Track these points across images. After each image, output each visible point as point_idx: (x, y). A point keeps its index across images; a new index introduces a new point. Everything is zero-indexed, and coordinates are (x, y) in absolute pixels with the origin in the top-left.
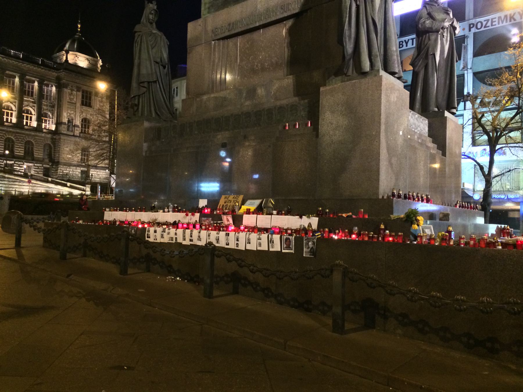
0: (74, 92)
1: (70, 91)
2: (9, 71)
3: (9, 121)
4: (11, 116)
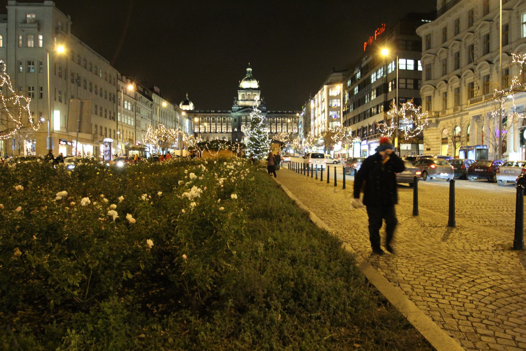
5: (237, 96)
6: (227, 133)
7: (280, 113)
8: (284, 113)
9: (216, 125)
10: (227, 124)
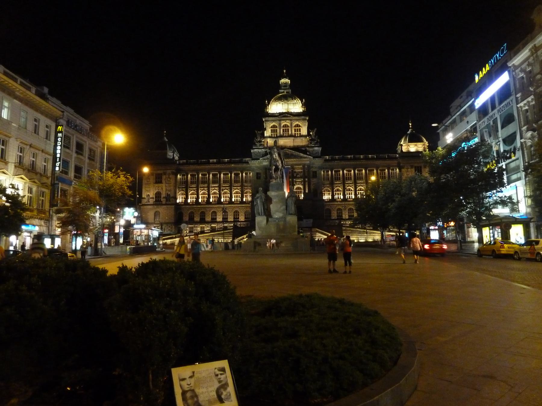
0: (409, 170)
1: (406, 170)
2: (368, 168)
4: (352, 194)
6: (242, 202)
7: (351, 159)
8: (359, 159)
9: (219, 187)
10: (242, 187)
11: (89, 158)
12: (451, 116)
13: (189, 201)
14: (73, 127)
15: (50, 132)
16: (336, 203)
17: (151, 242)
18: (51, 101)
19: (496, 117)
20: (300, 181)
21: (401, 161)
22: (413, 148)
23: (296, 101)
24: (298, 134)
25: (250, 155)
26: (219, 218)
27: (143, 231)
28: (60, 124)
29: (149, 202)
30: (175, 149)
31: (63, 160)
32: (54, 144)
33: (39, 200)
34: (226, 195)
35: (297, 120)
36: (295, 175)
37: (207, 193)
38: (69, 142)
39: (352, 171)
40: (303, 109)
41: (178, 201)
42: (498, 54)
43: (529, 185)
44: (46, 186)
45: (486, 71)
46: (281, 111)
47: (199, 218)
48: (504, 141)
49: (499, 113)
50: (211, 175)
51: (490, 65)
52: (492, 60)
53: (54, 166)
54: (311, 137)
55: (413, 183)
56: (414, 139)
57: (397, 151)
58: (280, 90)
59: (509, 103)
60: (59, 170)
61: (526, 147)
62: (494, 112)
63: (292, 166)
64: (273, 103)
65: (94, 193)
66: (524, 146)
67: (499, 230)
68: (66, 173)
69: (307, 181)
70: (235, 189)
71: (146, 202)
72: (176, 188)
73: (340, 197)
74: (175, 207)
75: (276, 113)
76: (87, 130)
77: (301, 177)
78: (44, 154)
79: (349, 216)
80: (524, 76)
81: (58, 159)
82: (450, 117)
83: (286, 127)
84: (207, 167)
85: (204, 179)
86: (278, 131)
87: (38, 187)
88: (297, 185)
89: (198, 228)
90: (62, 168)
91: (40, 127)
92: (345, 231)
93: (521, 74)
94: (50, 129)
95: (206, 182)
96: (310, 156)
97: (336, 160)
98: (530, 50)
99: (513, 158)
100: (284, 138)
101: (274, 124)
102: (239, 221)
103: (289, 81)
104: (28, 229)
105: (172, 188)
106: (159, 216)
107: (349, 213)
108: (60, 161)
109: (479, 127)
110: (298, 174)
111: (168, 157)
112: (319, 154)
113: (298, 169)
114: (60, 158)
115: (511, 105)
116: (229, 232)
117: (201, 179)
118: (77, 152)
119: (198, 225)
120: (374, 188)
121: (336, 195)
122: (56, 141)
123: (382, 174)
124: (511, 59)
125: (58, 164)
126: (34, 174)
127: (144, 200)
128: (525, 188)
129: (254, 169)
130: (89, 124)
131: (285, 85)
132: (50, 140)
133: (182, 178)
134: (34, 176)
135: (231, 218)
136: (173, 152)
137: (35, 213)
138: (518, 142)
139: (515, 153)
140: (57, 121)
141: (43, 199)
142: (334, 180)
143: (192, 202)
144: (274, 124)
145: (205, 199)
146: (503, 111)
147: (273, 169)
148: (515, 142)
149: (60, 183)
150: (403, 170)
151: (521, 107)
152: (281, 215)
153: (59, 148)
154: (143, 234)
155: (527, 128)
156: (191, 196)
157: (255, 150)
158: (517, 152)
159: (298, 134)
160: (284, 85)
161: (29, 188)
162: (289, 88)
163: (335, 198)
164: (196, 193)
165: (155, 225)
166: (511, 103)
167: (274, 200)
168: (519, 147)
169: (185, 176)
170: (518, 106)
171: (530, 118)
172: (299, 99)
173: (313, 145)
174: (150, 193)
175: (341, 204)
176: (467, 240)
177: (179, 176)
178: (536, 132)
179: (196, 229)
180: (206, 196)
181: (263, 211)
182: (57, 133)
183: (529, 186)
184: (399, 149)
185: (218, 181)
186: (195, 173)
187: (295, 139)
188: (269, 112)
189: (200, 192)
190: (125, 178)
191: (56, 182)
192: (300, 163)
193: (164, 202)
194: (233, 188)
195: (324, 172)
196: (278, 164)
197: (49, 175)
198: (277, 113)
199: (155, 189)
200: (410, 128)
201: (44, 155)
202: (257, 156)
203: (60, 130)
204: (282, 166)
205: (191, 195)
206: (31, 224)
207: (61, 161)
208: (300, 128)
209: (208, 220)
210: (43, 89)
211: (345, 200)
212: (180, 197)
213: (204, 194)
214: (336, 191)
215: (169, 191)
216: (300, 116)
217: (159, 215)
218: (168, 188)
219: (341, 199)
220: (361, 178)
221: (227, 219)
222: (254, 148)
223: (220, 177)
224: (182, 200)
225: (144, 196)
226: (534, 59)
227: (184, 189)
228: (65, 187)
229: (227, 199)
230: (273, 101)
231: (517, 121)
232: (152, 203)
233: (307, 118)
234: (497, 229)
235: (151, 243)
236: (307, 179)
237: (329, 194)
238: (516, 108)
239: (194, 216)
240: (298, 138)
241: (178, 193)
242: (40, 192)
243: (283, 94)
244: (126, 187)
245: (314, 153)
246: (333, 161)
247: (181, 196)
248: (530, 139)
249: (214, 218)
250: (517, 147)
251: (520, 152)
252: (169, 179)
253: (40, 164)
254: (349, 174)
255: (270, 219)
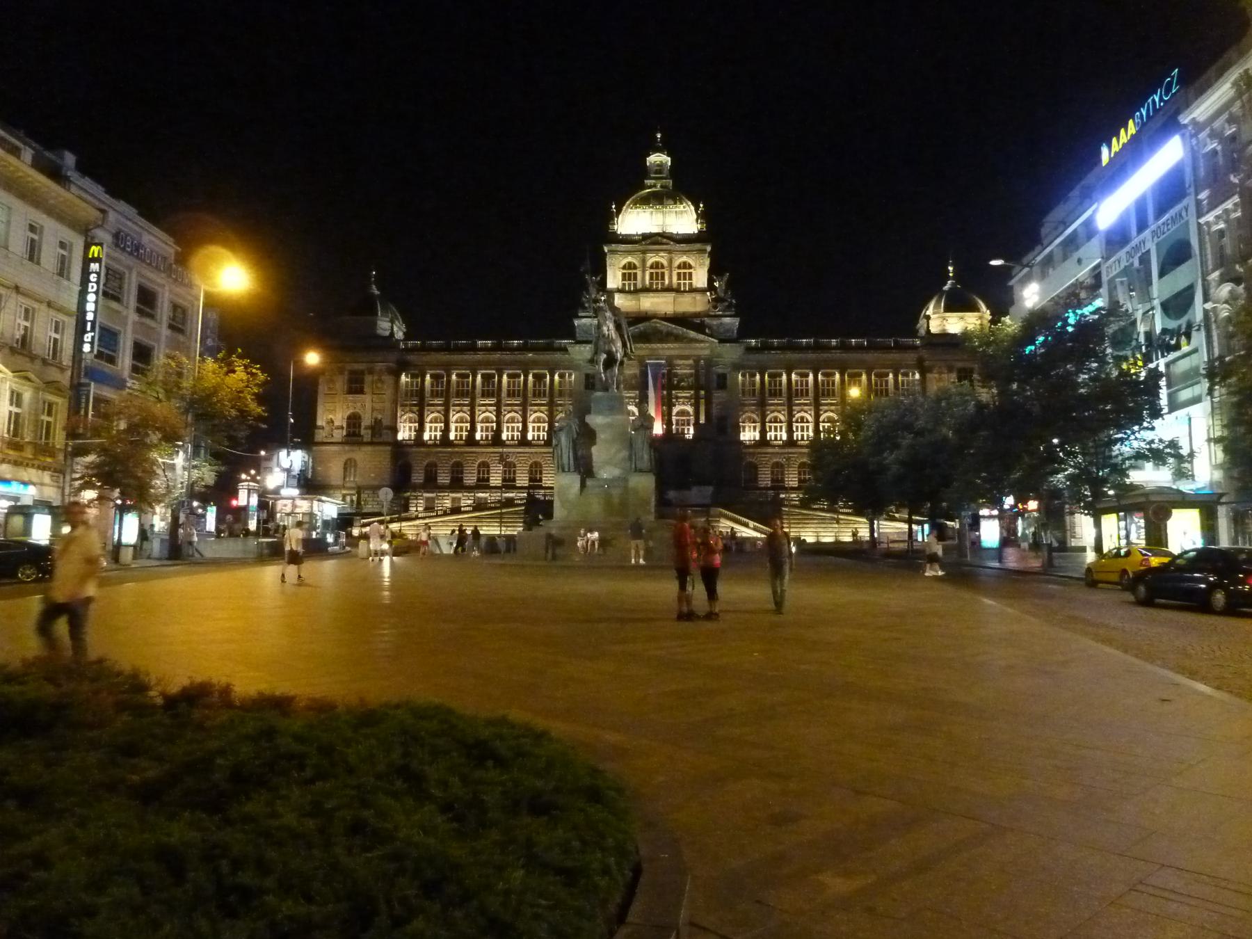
1: (936, 376)
3: (805, 439)
4: (808, 430)
5: (601, 270)
7: (808, 348)
8: (828, 348)
9: (498, 405)
10: (551, 405)
11: (171, 327)
12: (1042, 245)
13: (426, 436)
14: (129, 250)
15: (70, 257)
16: (770, 450)
17: (318, 531)
18: (75, 184)
19: (1147, 249)
20: (688, 395)
21: (924, 353)
22: (955, 324)
23: (684, 207)
24: (685, 284)
25: (570, 333)
26: (496, 480)
27: (299, 502)
28: (97, 241)
29: (332, 436)
30: (396, 315)
31: (102, 328)
32: (80, 288)
33: (37, 423)
34: (513, 425)
35: (684, 252)
36: (675, 382)
37: (469, 418)
38: (121, 287)
39: (811, 377)
40: (699, 226)
41: (400, 437)
42: (1157, 95)
43: (1221, 414)
44: (60, 390)
45: (1129, 137)
46: (647, 231)
47: (449, 478)
48: (1165, 307)
49: (1155, 238)
50: (479, 378)
51: (1138, 123)
52: (1142, 109)
53: (79, 342)
54: (716, 293)
55: (943, 404)
56: (958, 304)
57: (917, 331)
58: (646, 181)
59: (1180, 215)
60: (92, 351)
61: (1215, 321)
62: (1142, 236)
63: (670, 360)
64: (629, 210)
65: (166, 409)
66: (1213, 320)
67: (1142, 523)
68: (111, 360)
69: (703, 396)
70: (535, 412)
71: (326, 437)
72: (397, 404)
73: (781, 435)
74: (391, 451)
75: (634, 235)
76: (165, 259)
77: (689, 388)
78: (52, 313)
79: (800, 481)
80: (1219, 148)
81: (89, 324)
82: (1038, 248)
83: (657, 267)
84: (469, 357)
85: (463, 386)
86: (639, 277)
87: (37, 389)
88: (679, 404)
89: (446, 501)
90: (99, 346)
91: (45, 247)
92: (787, 515)
93: (1212, 144)
94: (70, 252)
95: (467, 393)
96: (711, 336)
97: (771, 348)
98: (1235, 84)
99: (1185, 348)
100: (651, 294)
101: (630, 259)
102: (541, 487)
103: (669, 159)
104: (8, 493)
105: (388, 405)
106: (355, 471)
107: (799, 474)
108: (93, 329)
109: (1107, 272)
110: (683, 381)
111: (380, 332)
112: (733, 332)
113: (684, 369)
114: (93, 323)
115: (1186, 219)
116: (516, 513)
117: (455, 386)
118: (139, 311)
119: (447, 494)
120: (852, 417)
121: (770, 431)
122: (85, 281)
123: (881, 385)
124: (1187, 104)
125: (88, 338)
126: (27, 359)
127: (321, 431)
128: (1211, 423)
129: (580, 365)
130: (174, 246)
131: (658, 168)
132: (68, 279)
133: (412, 382)
134: (21, 361)
135: (522, 480)
136: (392, 322)
137: (28, 453)
138: (1198, 309)
139: (1188, 336)
140: (89, 234)
141: (50, 419)
142: (767, 395)
143: (433, 438)
144: (630, 259)
145: (465, 434)
146: (1164, 233)
147: (602, 360)
148: (1192, 307)
149: (92, 384)
150: (929, 376)
151: (1208, 223)
152: (616, 472)
153: (91, 297)
154: (297, 510)
155: (1221, 275)
156: (431, 425)
157: (584, 320)
158: (1194, 334)
159: (685, 284)
160: (656, 170)
161: (12, 392)
162: (669, 177)
163: (768, 438)
164: (443, 418)
165: (344, 492)
166: (1184, 214)
167: (601, 436)
168: (1201, 322)
169: (417, 378)
170: (1202, 221)
171: (1228, 251)
172: (690, 203)
173: (721, 313)
174: (335, 415)
175: (782, 453)
176: (1069, 545)
177: (403, 378)
178: (1243, 286)
179: (440, 504)
180: (467, 427)
181: (572, 462)
182: (87, 261)
183: (1221, 416)
184: (922, 326)
185: (496, 391)
186: (442, 372)
187: (678, 297)
188: (619, 233)
189: (453, 416)
190: (248, 373)
191: (83, 380)
192: (687, 352)
193: (367, 438)
194: (530, 408)
195: (744, 375)
196: (614, 349)
197: (64, 363)
198: (637, 235)
199: (348, 408)
200: (949, 278)
201: (54, 314)
202: (587, 335)
203: (96, 255)
204: (626, 354)
205: (431, 422)
206: (16, 480)
207: (97, 330)
208: (690, 271)
209: (469, 482)
210: (62, 158)
211: (791, 443)
212: (404, 427)
213: (461, 420)
214: (770, 422)
215: (380, 411)
216: (691, 243)
217: (356, 466)
218: (377, 406)
219: (783, 441)
220: (829, 393)
221: (514, 480)
222: (580, 314)
223: (500, 382)
224: (410, 435)
225: (320, 423)
226: (1243, 106)
227: (415, 409)
228: (108, 393)
229: (516, 434)
230: (629, 205)
231: (1198, 258)
232: (340, 441)
233: (709, 248)
234: (1136, 520)
235: (317, 534)
236: (703, 392)
237: (755, 428)
238: (1196, 225)
239: (436, 473)
240: (686, 294)
241: (401, 417)
242: (41, 402)
243: (654, 189)
244: (249, 397)
245: (722, 330)
246: (766, 352)
247: (408, 425)
248: (1226, 302)
249: (483, 477)
250: (1196, 322)
251: (1203, 333)
252: (379, 385)
253: (43, 335)
254: (802, 382)
255: (589, 482)
